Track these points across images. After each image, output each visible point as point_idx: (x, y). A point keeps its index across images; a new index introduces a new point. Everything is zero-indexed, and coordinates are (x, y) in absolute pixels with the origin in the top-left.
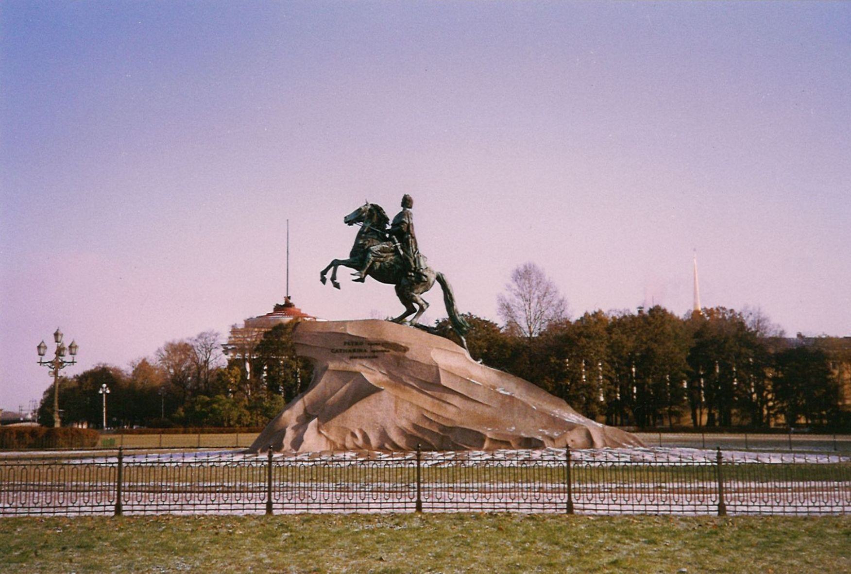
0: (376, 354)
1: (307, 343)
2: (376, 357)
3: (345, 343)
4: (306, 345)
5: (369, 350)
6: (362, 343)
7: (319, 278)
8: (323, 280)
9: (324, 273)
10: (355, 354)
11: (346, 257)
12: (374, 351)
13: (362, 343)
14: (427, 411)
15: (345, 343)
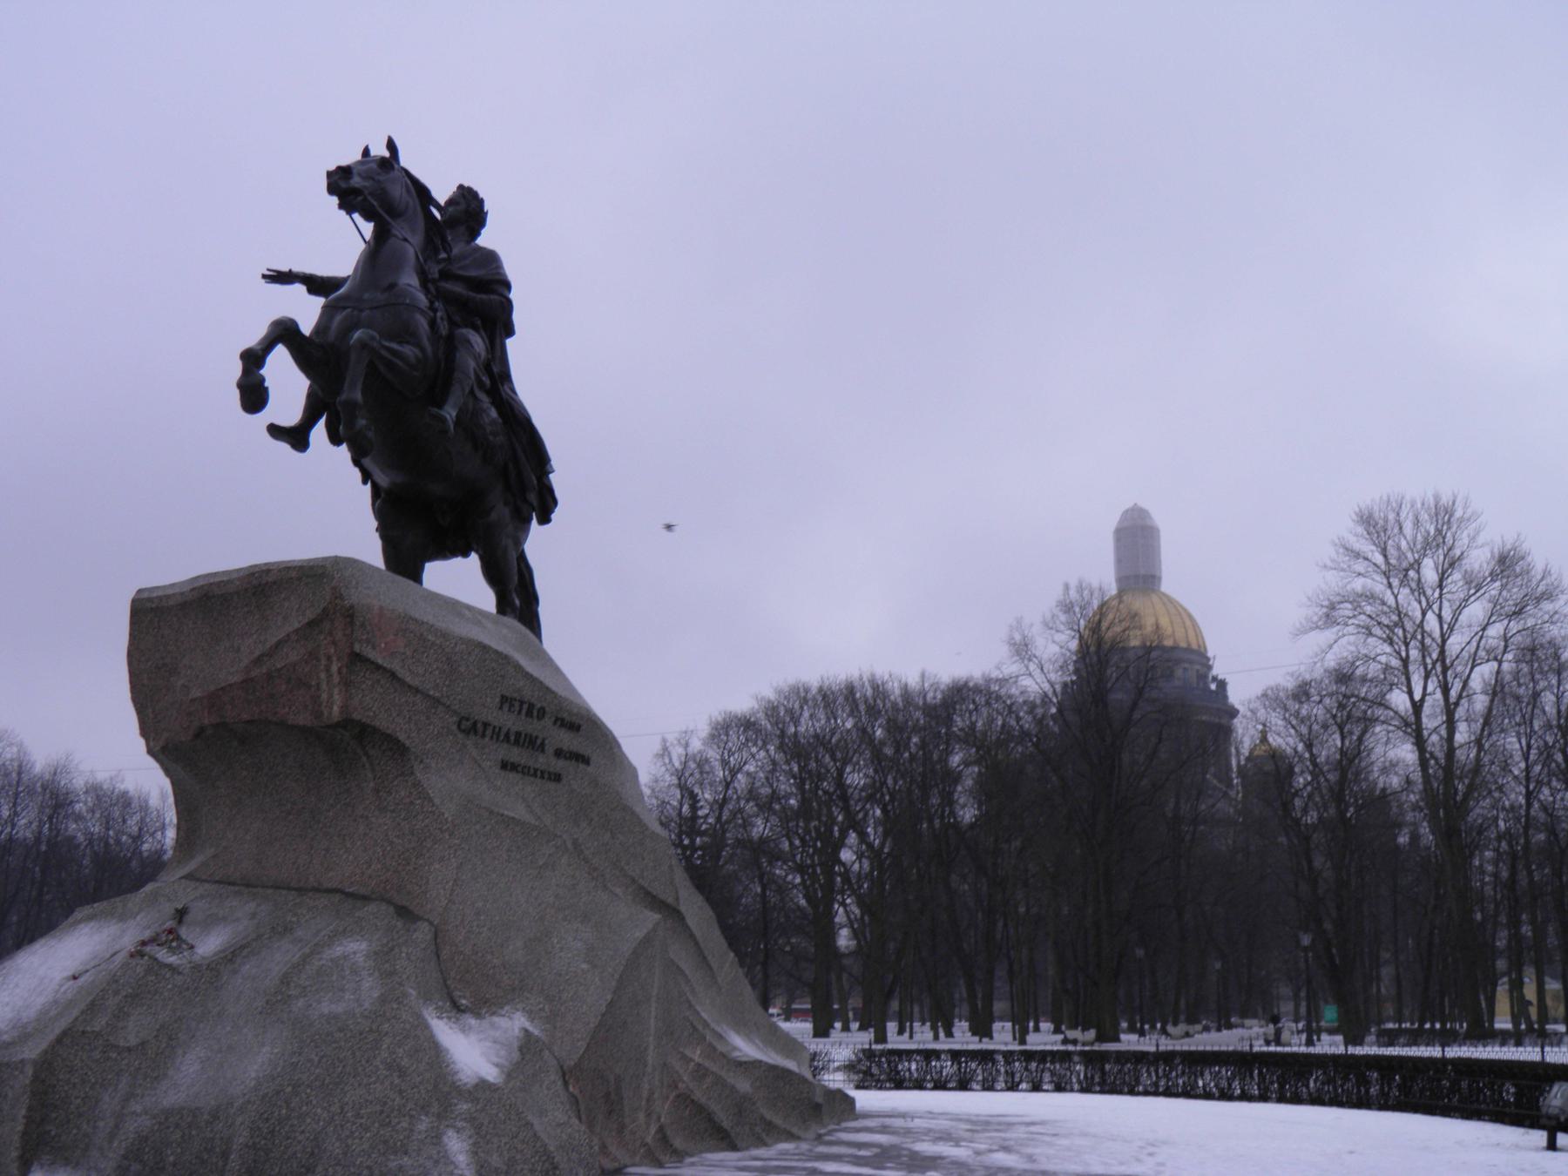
0: (559, 765)
1: (395, 665)
2: (557, 778)
3: (504, 699)
4: (393, 675)
5: (550, 750)
6: (542, 713)
7: (237, 369)
8: (253, 395)
9: (253, 360)
10: (516, 755)
11: (307, 328)
12: (559, 753)
13: (542, 713)
14: (691, 1006)
15: (504, 699)
